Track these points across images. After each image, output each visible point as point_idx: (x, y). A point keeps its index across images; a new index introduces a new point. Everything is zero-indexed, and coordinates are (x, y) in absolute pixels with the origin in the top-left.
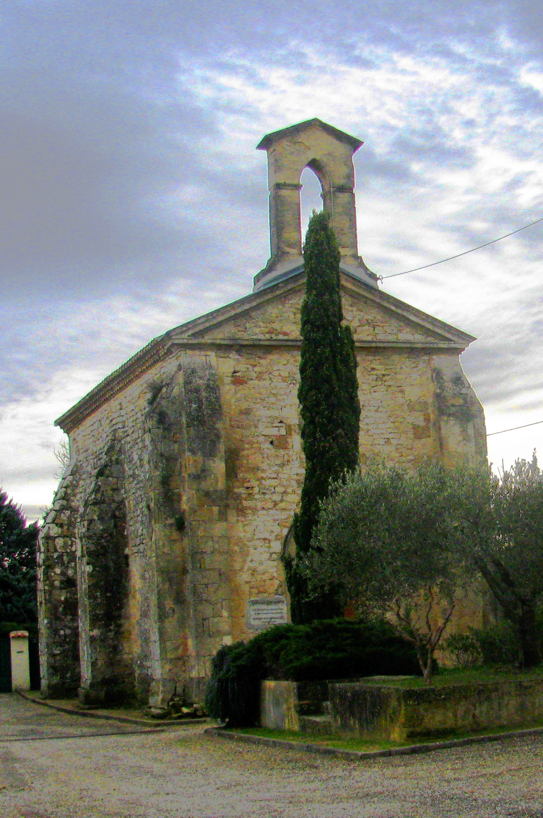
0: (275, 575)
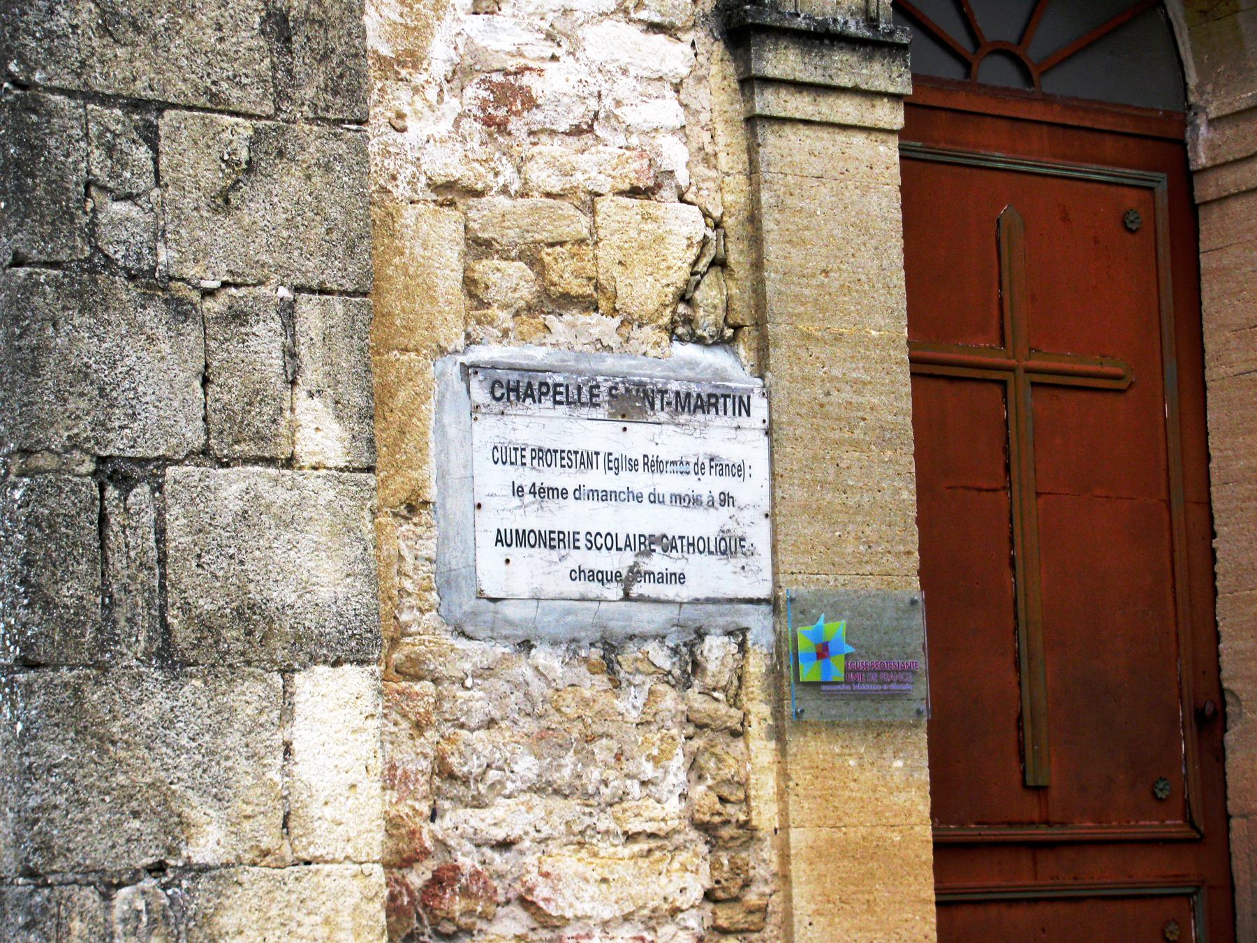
0: (675, 155)
